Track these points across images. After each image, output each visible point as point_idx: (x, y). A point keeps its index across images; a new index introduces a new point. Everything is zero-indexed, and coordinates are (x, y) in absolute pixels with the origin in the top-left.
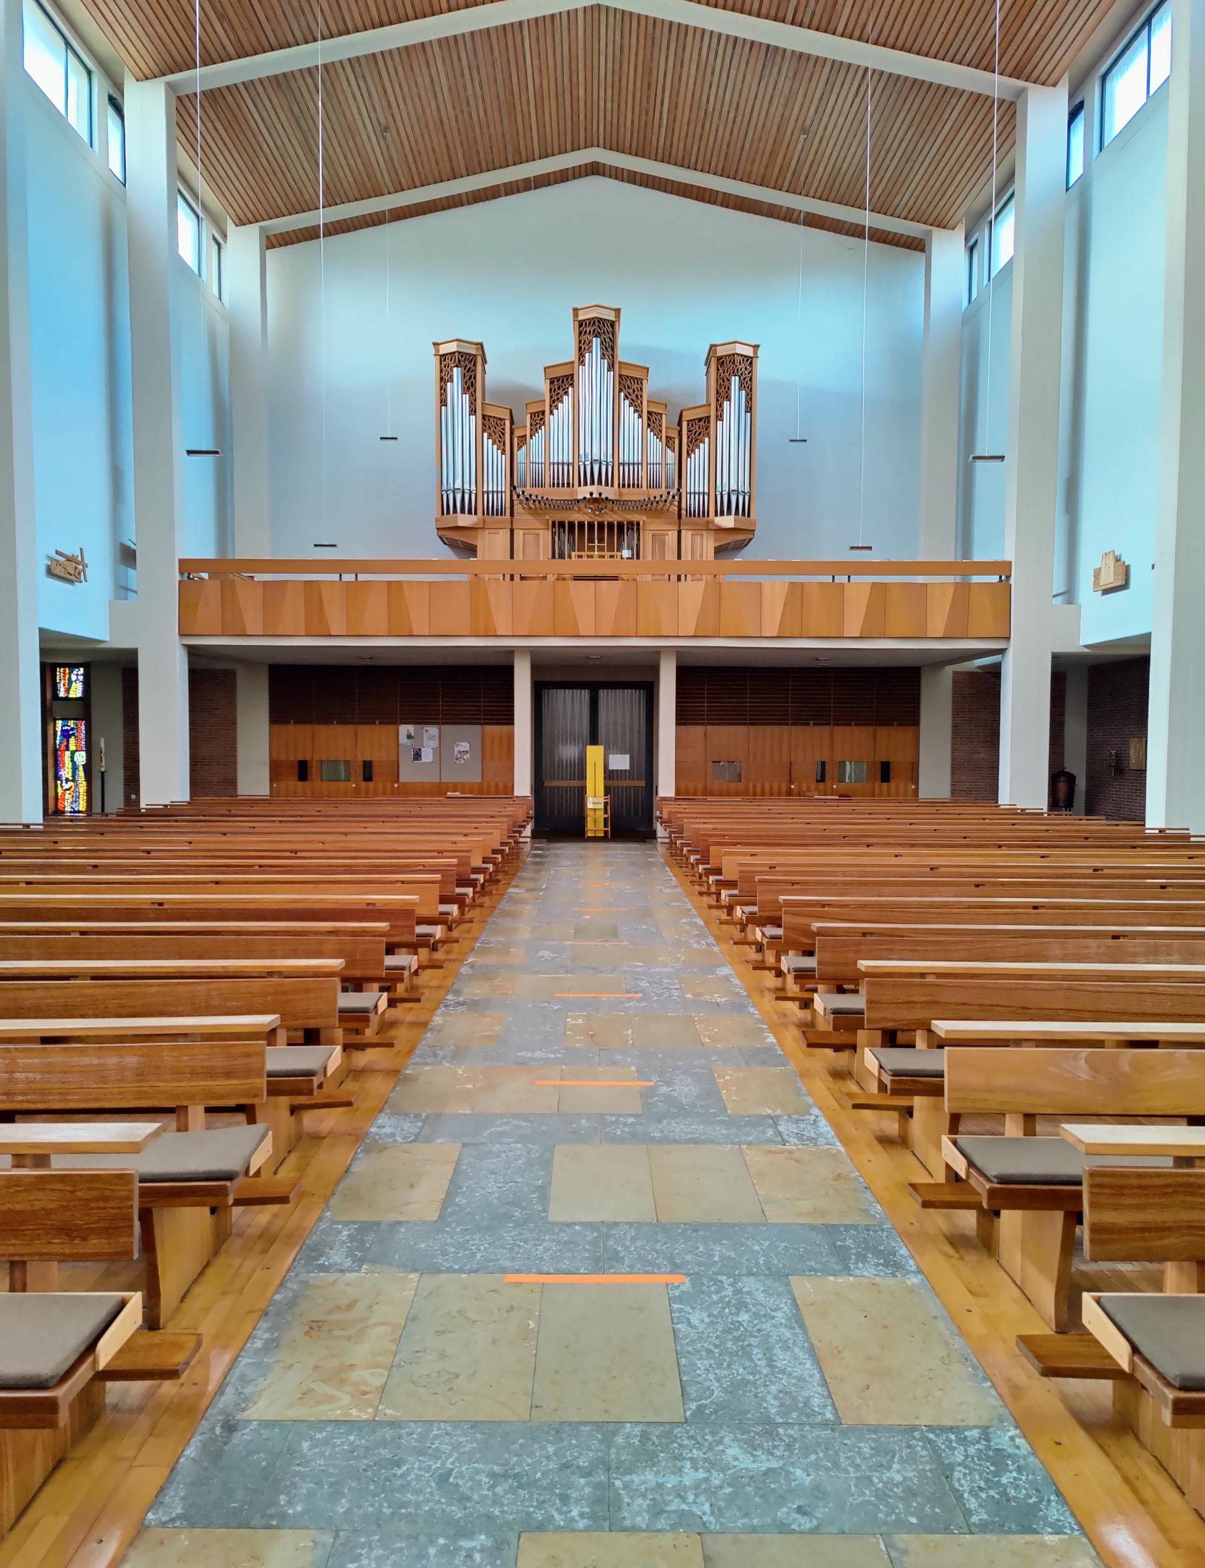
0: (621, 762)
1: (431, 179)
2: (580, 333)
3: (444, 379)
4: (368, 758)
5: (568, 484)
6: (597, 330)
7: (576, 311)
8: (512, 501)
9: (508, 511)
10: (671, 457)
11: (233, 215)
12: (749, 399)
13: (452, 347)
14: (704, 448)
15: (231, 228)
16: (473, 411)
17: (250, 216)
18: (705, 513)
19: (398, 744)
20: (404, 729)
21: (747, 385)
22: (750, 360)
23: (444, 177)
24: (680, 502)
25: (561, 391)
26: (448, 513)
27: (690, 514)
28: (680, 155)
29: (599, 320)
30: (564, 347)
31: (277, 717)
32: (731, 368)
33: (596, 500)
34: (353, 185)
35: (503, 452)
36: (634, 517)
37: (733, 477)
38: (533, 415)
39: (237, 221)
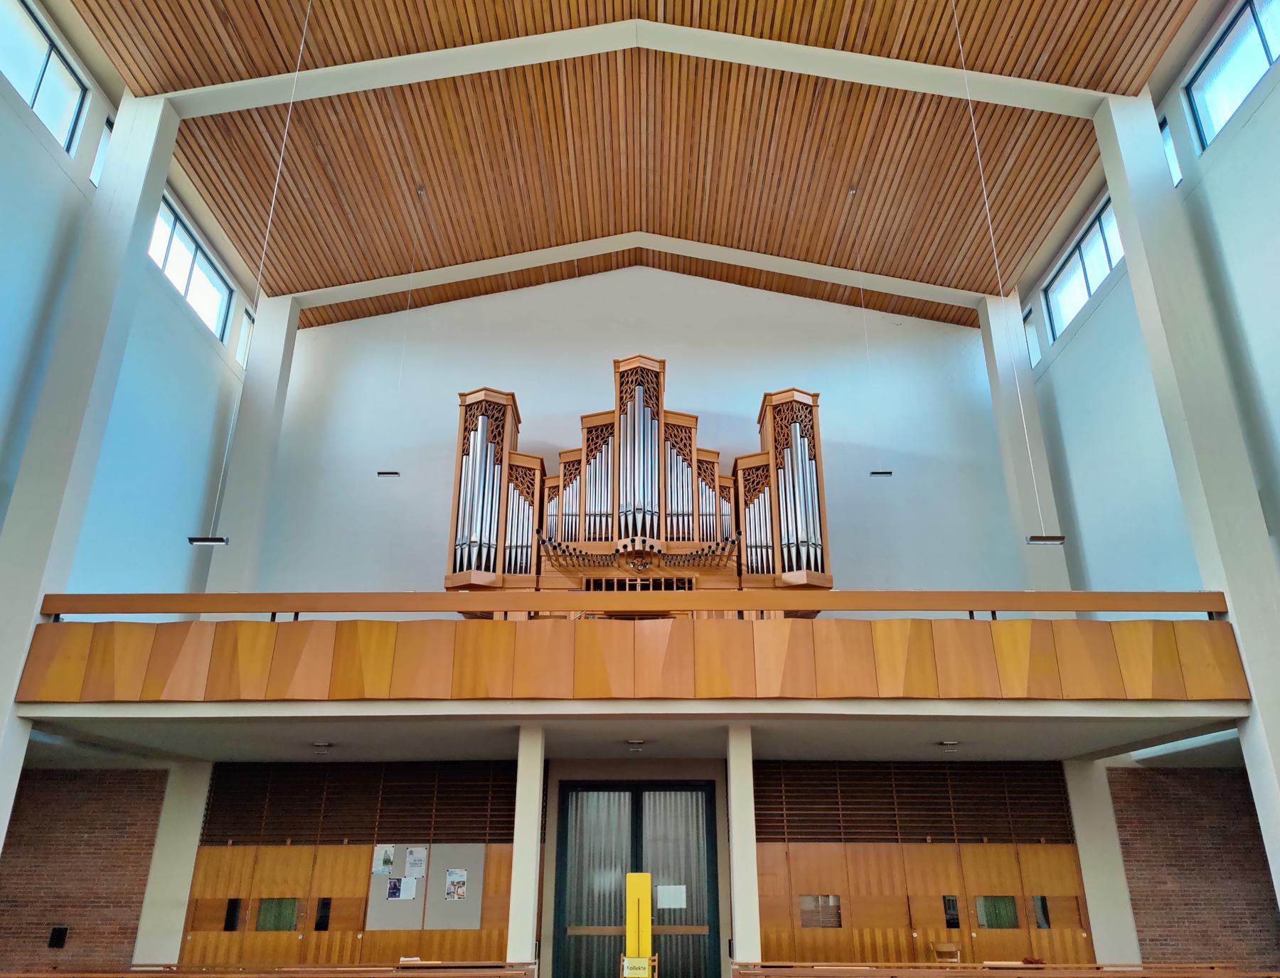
0: (674, 897)
1: (472, 256)
2: (622, 384)
3: (468, 429)
4: (325, 895)
5: (607, 539)
6: (642, 382)
7: (616, 363)
8: (539, 557)
9: (534, 568)
10: (727, 508)
12: (813, 446)
13: (481, 396)
14: (762, 501)
15: (263, 297)
16: (498, 460)
17: (282, 284)
18: (770, 570)
19: (370, 873)
20: (382, 850)
21: (810, 432)
22: (810, 409)
23: (486, 254)
24: (739, 557)
25: (600, 442)
26: (461, 569)
27: (752, 570)
28: (723, 233)
29: (642, 369)
30: (604, 399)
31: (212, 835)
32: (789, 417)
33: (639, 554)
34: (391, 256)
35: (532, 504)
36: (686, 574)
38: (567, 464)
39: (269, 291)
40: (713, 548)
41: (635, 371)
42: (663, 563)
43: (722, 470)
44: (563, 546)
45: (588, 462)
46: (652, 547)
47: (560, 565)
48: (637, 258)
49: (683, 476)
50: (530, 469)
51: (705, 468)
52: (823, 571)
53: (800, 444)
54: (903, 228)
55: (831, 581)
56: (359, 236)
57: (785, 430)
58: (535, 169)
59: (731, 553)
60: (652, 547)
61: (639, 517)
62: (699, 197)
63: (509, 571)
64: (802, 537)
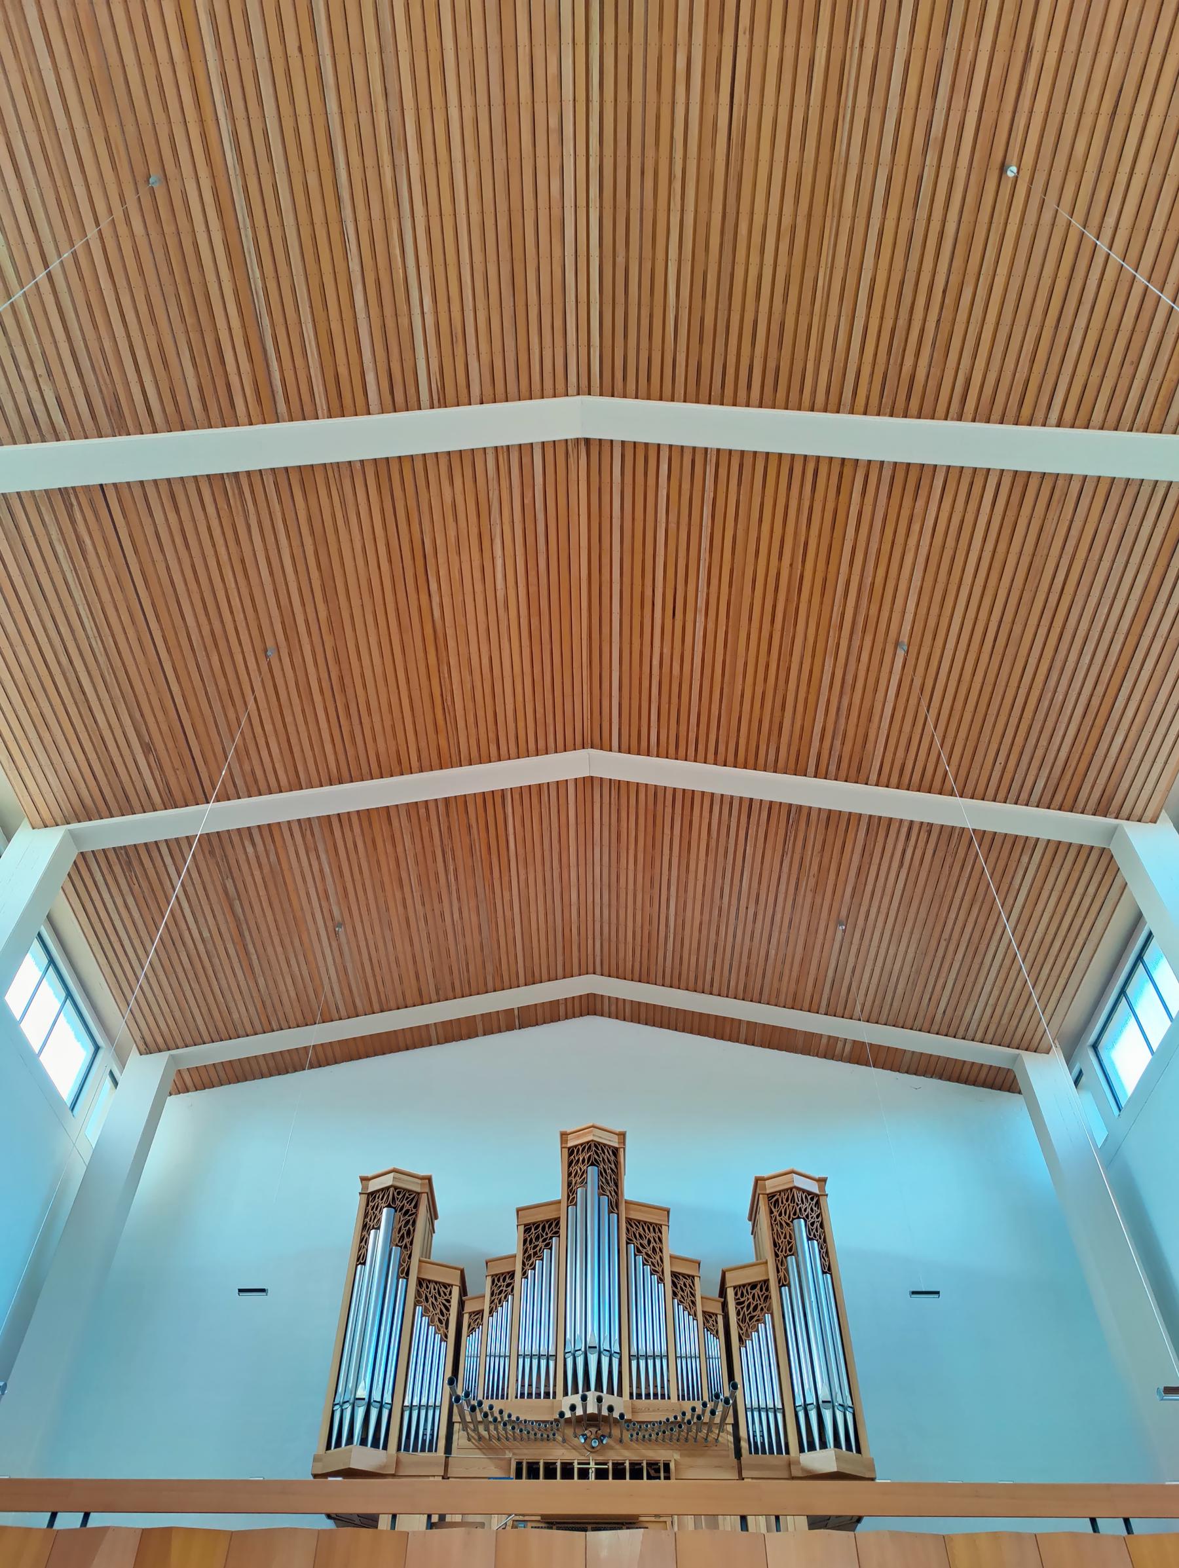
1: (393, 1004)
2: (570, 1164)
3: (368, 1225)
5: (547, 1395)
6: (595, 1161)
7: (564, 1136)
10: (716, 1347)
11: (138, 1038)
12: (825, 1254)
13: (388, 1181)
14: (763, 1334)
15: (134, 1056)
17: (160, 1040)
21: (819, 1232)
22: (816, 1199)
23: (409, 1002)
24: (736, 1426)
25: (541, 1244)
26: (338, 1444)
27: (755, 1449)
30: (546, 1184)
32: (790, 1209)
33: (592, 1420)
34: (296, 1004)
36: (660, 1454)
37: (817, 1380)
38: (496, 1278)
39: (143, 1047)
40: (699, 1410)
41: (588, 1146)
42: (627, 1435)
43: (705, 1287)
44: (485, 1407)
45: (524, 1274)
46: (611, 1409)
47: (480, 1438)
48: (589, 1006)
49: (655, 1296)
50: (446, 1286)
51: (682, 1285)
52: (859, 1451)
53: (808, 1249)
54: (906, 970)
55: (871, 1467)
56: (261, 981)
57: (787, 1229)
58: (473, 904)
59: (724, 1418)
60: (611, 1409)
61: (593, 1359)
62: (662, 934)
63: (407, 1449)
64: (824, 1394)
